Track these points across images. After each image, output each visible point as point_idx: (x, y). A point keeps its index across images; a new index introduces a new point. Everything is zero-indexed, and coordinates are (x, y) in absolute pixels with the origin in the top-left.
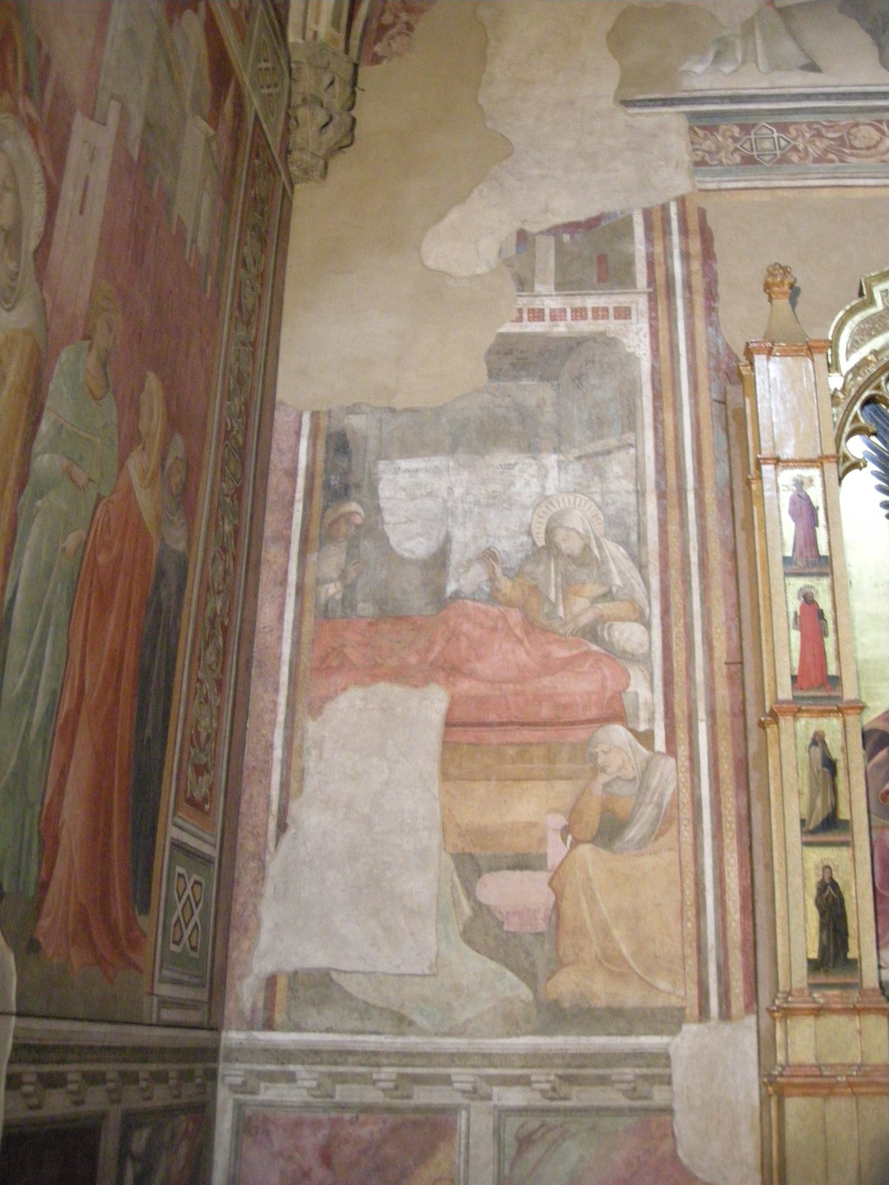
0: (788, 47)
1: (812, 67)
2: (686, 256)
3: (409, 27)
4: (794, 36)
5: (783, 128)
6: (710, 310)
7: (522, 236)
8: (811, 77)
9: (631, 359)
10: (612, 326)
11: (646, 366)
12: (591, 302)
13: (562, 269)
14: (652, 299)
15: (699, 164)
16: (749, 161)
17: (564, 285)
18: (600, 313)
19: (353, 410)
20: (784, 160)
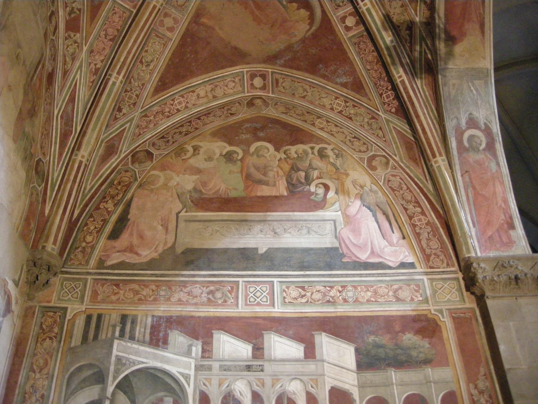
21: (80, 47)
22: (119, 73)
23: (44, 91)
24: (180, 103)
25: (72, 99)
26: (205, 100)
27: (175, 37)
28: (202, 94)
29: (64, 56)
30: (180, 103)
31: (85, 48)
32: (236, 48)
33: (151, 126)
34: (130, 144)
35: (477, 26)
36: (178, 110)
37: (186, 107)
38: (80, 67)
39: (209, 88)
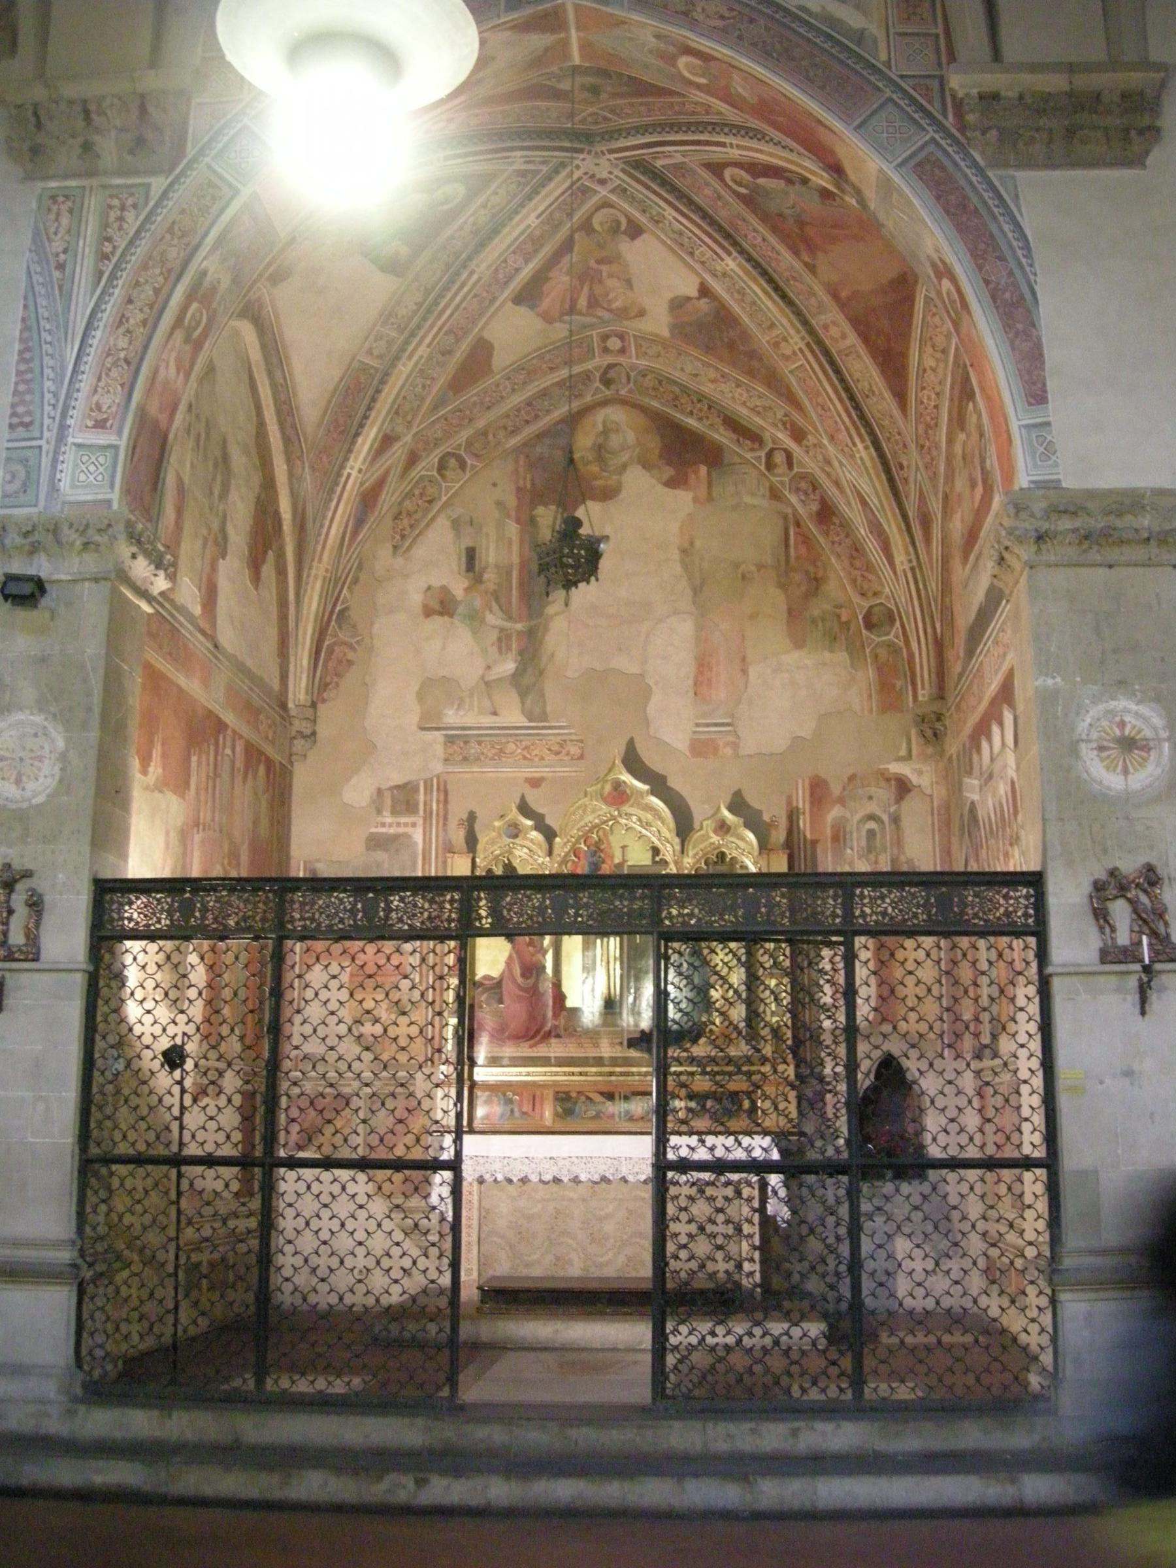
0: (487, 703)
1: (495, 713)
2: (438, 801)
3: (337, 684)
4: (490, 697)
5: (479, 743)
6: (445, 825)
7: (379, 791)
8: (494, 718)
9: (416, 844)
10: (409, 830)
11: (420, 846)
12: (403, 820)
13: (393, 807)
14: (425, 819)
15: (446, 760)
16: (465, 759)
17: (394, 812)
18: (406, 824)
19: (318, 861)
20: (478, 759)
21: (819, 445)
22: (854, 444)
23: (822, 540)
24: (929, 399)
25: (864, 503)
26: (942, 365)
27: (852, 339)
28: (932, 363)
29: (823, 470)
30: (929, 399)
31: (826, 442)
32: (892, 283)
33: (935, 453)
34: (936, 494)
35: (821, 129)
36: (936, 407)
37: (937, 394)
38: (840, 463)
39: (929, 350)
